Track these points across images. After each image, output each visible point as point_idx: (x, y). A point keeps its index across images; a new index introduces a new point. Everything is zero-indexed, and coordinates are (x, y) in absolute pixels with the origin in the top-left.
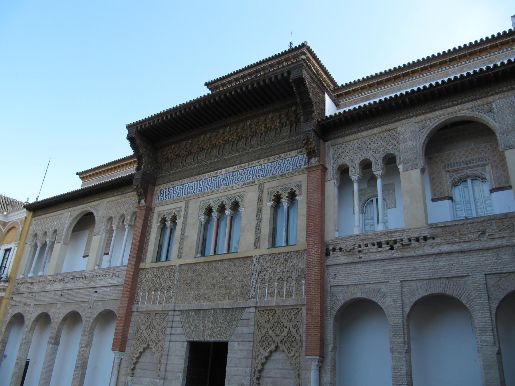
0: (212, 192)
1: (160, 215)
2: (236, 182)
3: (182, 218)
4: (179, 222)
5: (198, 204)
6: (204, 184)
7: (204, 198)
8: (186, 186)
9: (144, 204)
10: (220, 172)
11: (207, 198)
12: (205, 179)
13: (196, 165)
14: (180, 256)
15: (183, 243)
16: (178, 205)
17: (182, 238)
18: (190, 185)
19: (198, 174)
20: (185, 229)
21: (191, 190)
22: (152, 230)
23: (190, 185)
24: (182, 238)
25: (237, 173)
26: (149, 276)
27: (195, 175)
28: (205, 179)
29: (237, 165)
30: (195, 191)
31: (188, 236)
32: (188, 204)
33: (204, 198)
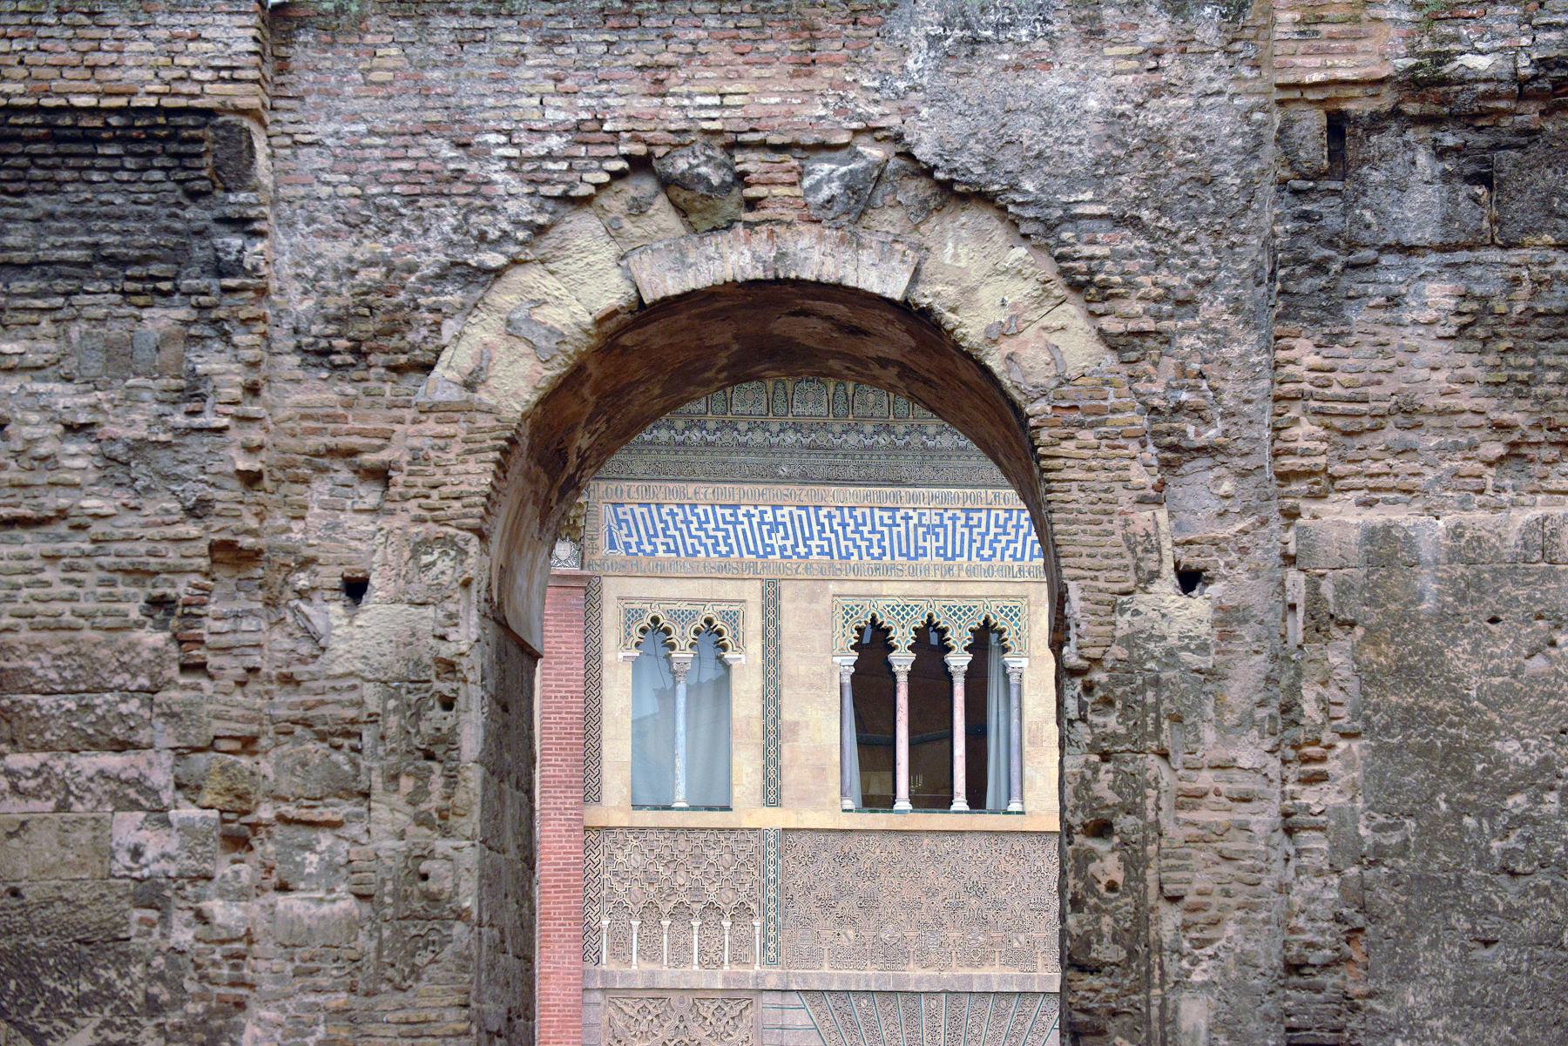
0: (884, 573)
1: (632, 615)
2: (986, 552)
3: (755, 647)
4: (746, 660)
5: (825, 604)
6: (840, 529)
7: (848, 588)
8: (749, 515)
9: (573, 568)
10: (912, 498)
11: (862, 588)
12: (840, 508)
13: (790, 437)
14: (772, 794)
15: (778, 750)
16: (728, 590)
17: (773, 735)
18: (769, 518)
19: (806, 479)
20: (778, 694)
21: (777, 540)
22: (605, 675)
23: (769, 518)
24: (773, 735)
25: (984, 515)
26: (631, 857)
27: (789, 479)
28: (840, 508)
29: (985, 486)
30: (802, 550)
31: (797, 724)
32: (777, 594)
33: (848, 588)
